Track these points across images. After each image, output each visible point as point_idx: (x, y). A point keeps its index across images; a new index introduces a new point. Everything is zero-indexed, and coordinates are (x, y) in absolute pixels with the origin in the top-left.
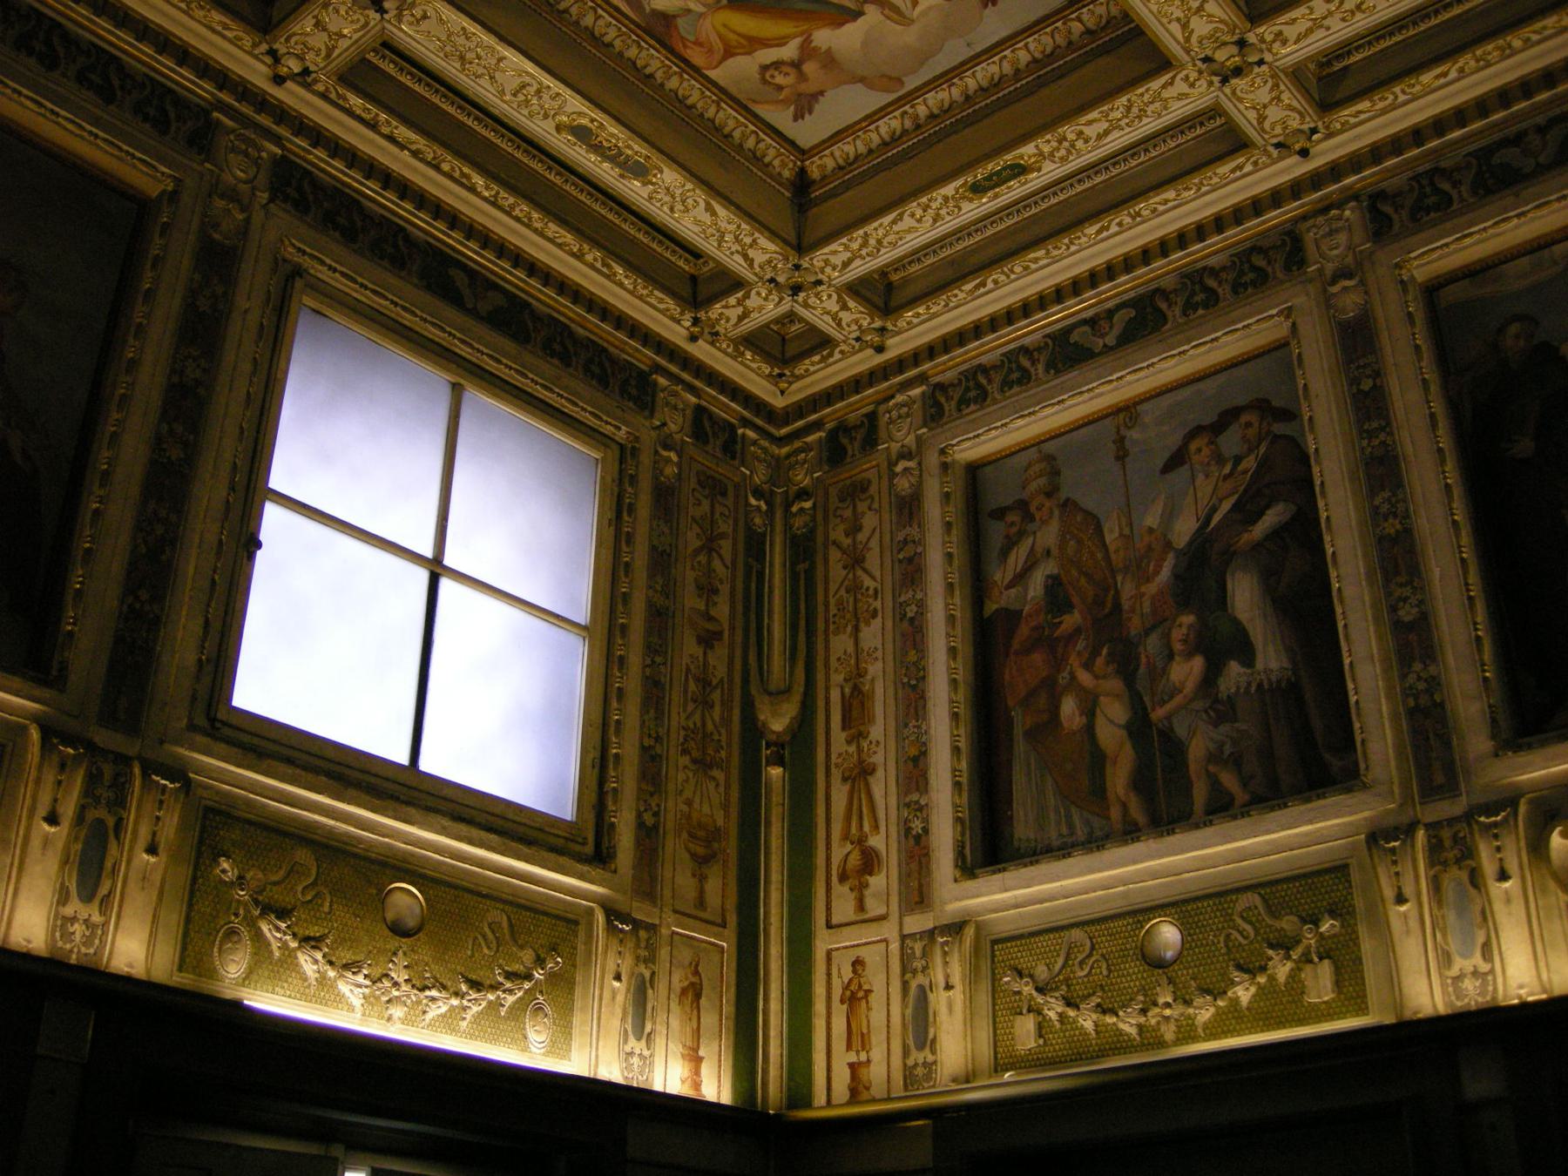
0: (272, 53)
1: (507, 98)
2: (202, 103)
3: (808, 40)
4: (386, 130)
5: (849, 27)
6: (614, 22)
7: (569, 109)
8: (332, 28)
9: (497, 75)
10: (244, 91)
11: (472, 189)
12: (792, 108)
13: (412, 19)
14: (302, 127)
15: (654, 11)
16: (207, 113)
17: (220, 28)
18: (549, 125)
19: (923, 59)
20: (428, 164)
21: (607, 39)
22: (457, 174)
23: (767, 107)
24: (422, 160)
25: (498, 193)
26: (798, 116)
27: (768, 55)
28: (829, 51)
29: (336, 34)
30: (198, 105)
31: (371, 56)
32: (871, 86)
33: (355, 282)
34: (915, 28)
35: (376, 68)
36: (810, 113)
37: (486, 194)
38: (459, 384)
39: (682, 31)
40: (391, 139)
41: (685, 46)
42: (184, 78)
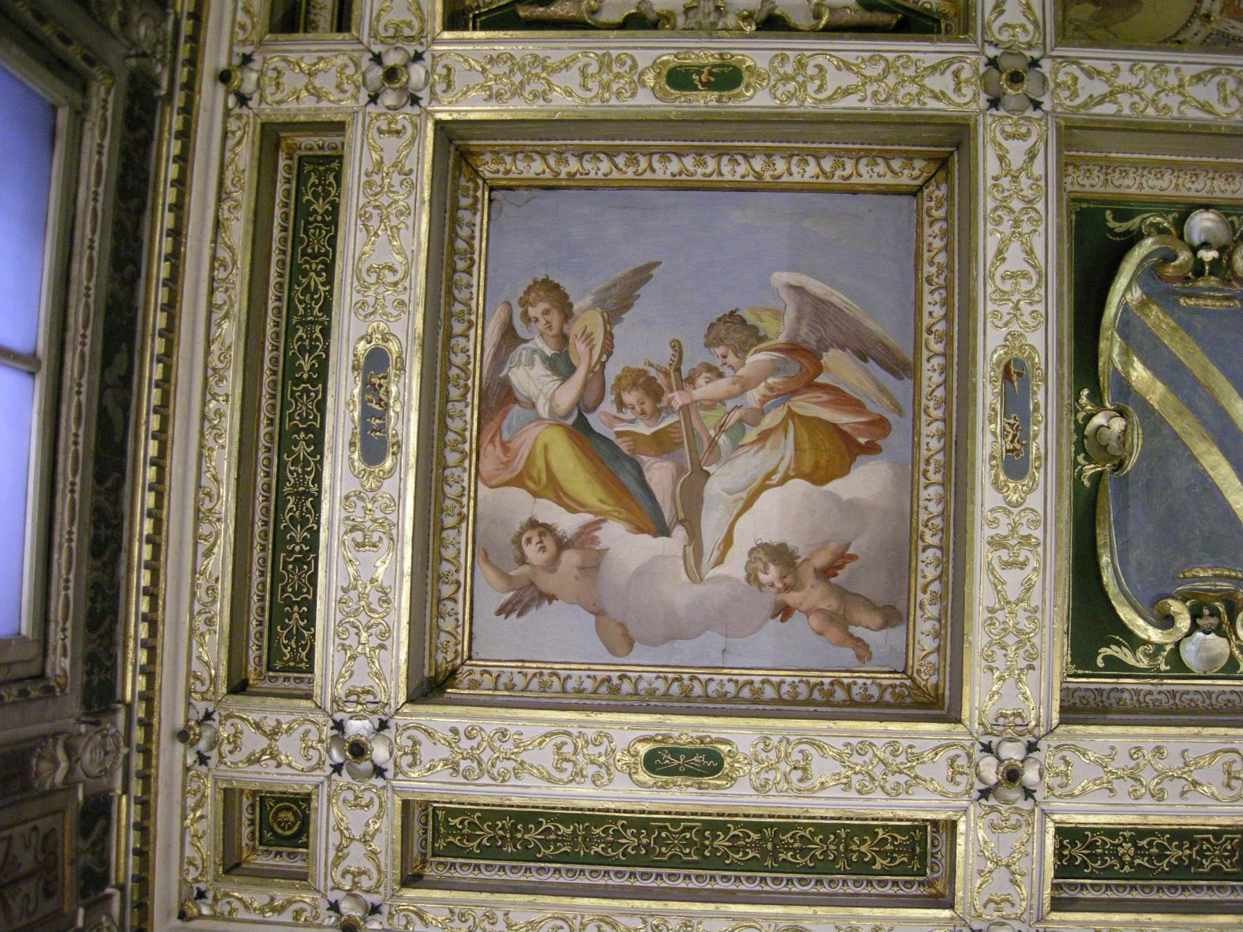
3: (596, 525)
5: (645, 538)
6: (471, 353)
12: (511, 594)
15: (507, 378)
19: (675, 633)
23: (491, 575)
26: (505, 610)
27: (549, 512)
28: (604, 552)
32: (600, 630)
33: (98, 184)
34: (698, 589)
36: (519, 615)
38: (39, 363)
39: (506, 422)
41: (492, 441)
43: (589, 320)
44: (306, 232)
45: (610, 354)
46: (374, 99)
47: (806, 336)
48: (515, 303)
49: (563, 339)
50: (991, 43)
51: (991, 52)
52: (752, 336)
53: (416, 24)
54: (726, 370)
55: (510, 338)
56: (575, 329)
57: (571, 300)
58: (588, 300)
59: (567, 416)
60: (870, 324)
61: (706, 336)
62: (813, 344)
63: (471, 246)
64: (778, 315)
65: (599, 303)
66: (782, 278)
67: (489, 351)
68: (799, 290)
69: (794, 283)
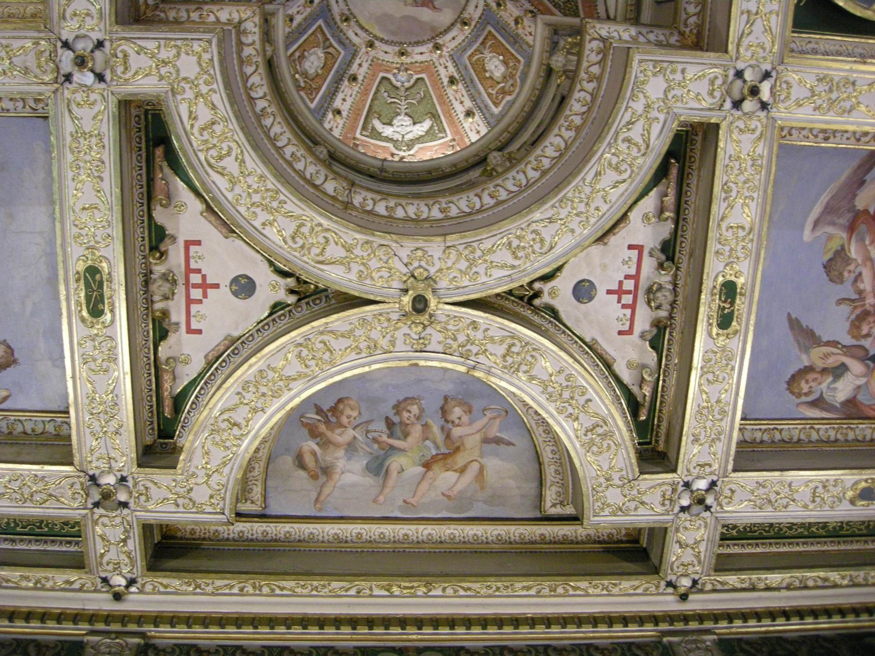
0: (670, 584)
1: (811, 507)
2: (653, 639)
4: (762, 586)
6: (828, 426)
7: (849, 485)
8: (691, 542)
9: (795, 496)
10: (671, 618)
11: (835, 586)
13: (727, 500)
14: (716, 617)
16: (660, 642)
17: (632, 592)
18: (846, 505)
20: (800, 588)
21: (832, 438)
22: (820, 583)
24: (796, 589)
25: (851, 576)
29: (695, 543)
30: (652, 642)
31: (722, 551)
35: (729, 555)
37: (845, 582)
39: (866, 403)
40: (768, 589)
42: (633, 632)
43: (816, 356)
44: (755, 531)
45: (838, 343)
46: (708, 508)
47: (844, 221)
48: (799, 401)
49: (824, 371)
50: (722, 105)
51: (728, 105)
52: (841, 255)
53: (664, 488)
54: (858, 270)
55: (818, 403)
56: (820, 364)
57: (802, 367)
58: (804, 357)
59: (867, 366)
60: (843, 178)
61: (836, 283)
62: (849, 216)
63: (766, 430)
64: (830, 237)
65: (806, 350)
66: (807, 235)
67: (825, 415)
68: (816, 223)
69: (811, 228)
